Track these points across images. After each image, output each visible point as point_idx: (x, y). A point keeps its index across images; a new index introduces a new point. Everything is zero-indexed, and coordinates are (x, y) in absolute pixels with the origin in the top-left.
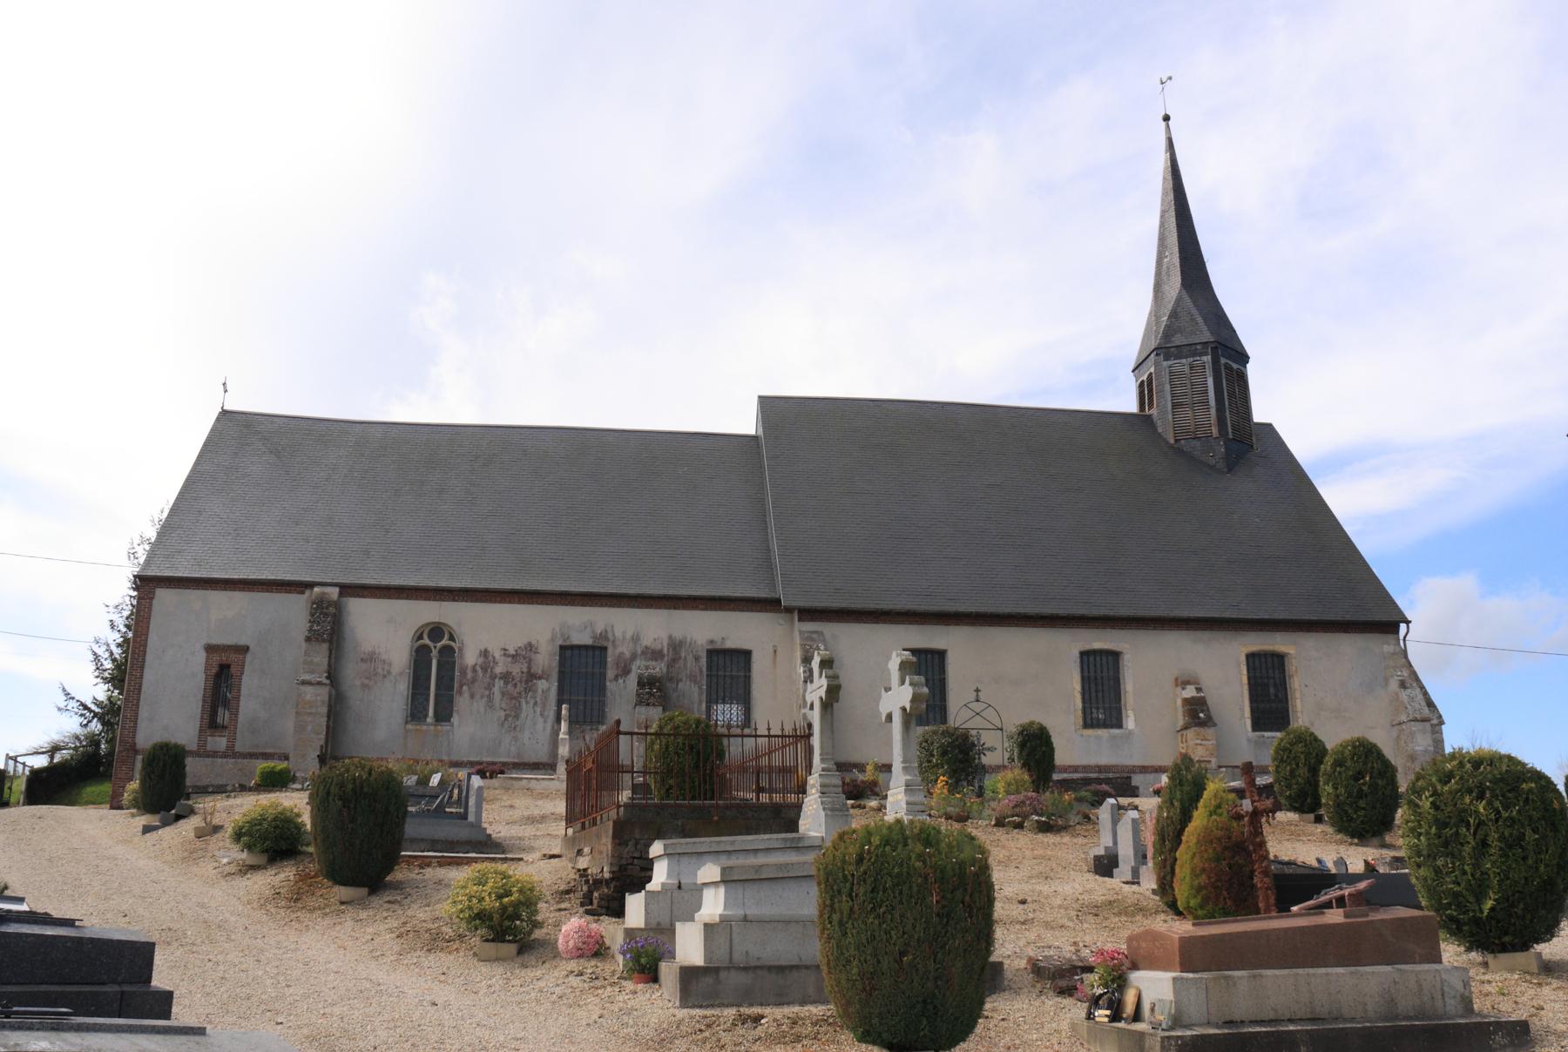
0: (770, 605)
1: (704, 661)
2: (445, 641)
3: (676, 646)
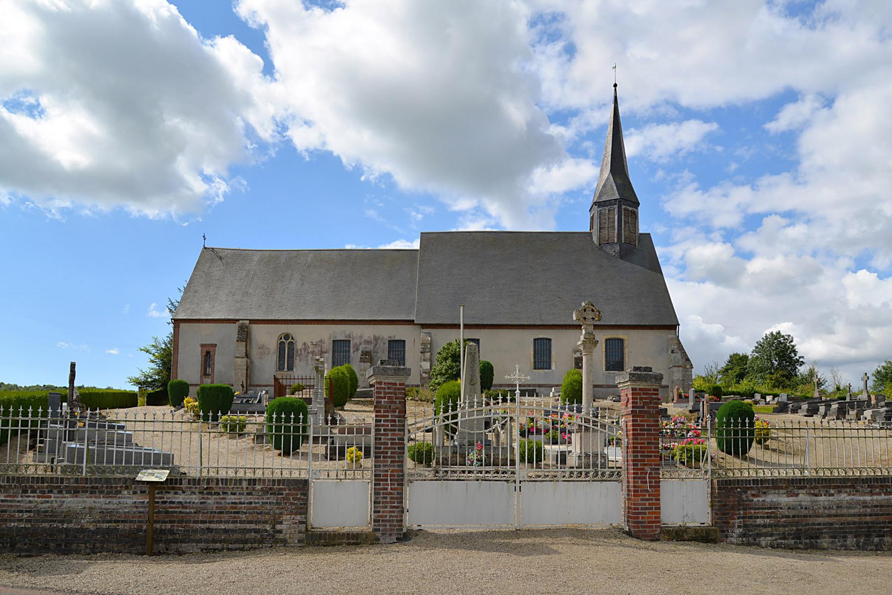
0: (411, 322)
1: (387, 345)
2: (290, 340)
3: (376, 339)
